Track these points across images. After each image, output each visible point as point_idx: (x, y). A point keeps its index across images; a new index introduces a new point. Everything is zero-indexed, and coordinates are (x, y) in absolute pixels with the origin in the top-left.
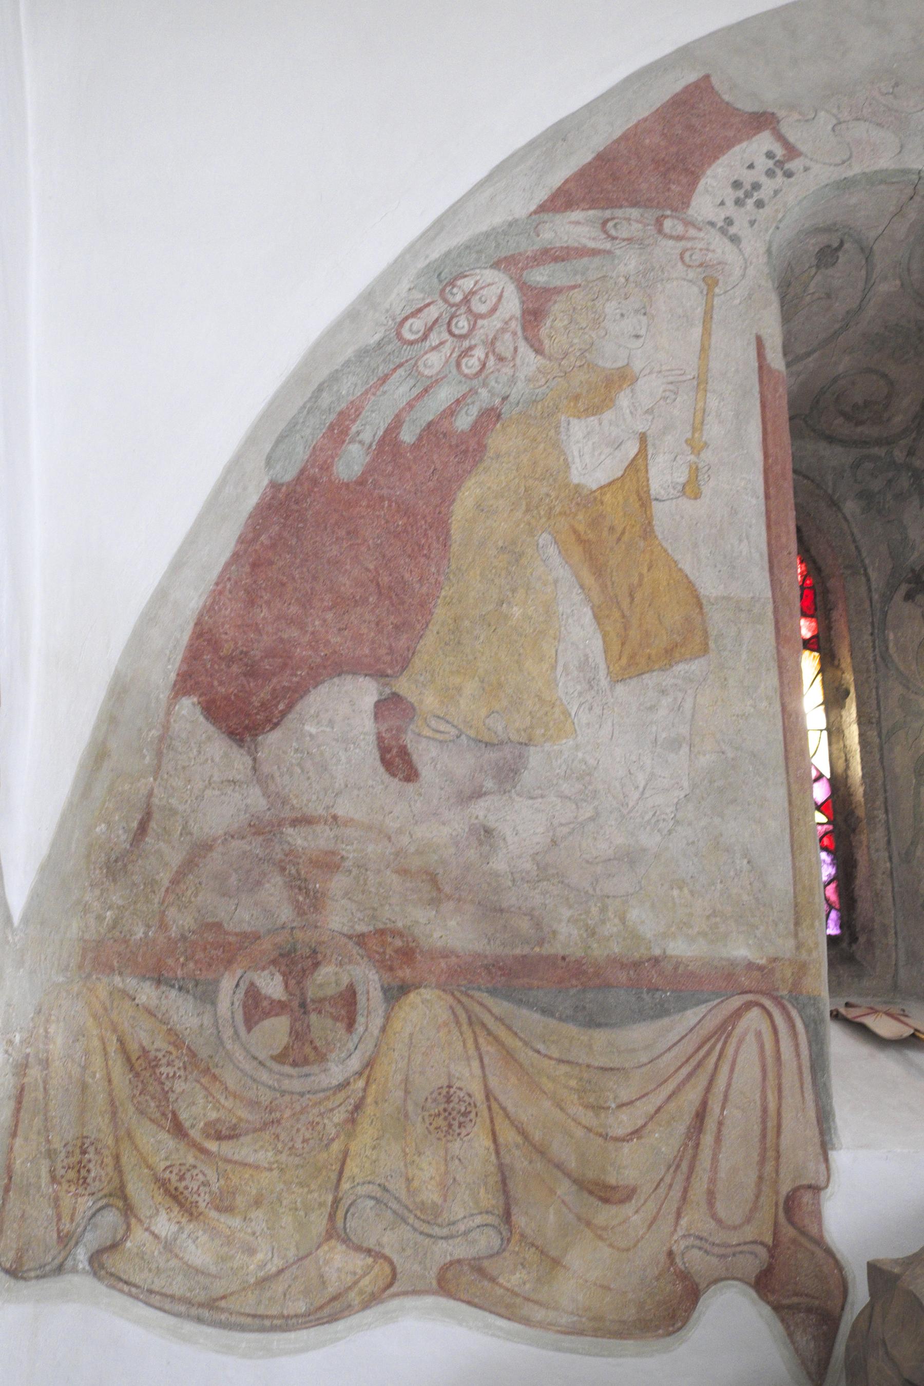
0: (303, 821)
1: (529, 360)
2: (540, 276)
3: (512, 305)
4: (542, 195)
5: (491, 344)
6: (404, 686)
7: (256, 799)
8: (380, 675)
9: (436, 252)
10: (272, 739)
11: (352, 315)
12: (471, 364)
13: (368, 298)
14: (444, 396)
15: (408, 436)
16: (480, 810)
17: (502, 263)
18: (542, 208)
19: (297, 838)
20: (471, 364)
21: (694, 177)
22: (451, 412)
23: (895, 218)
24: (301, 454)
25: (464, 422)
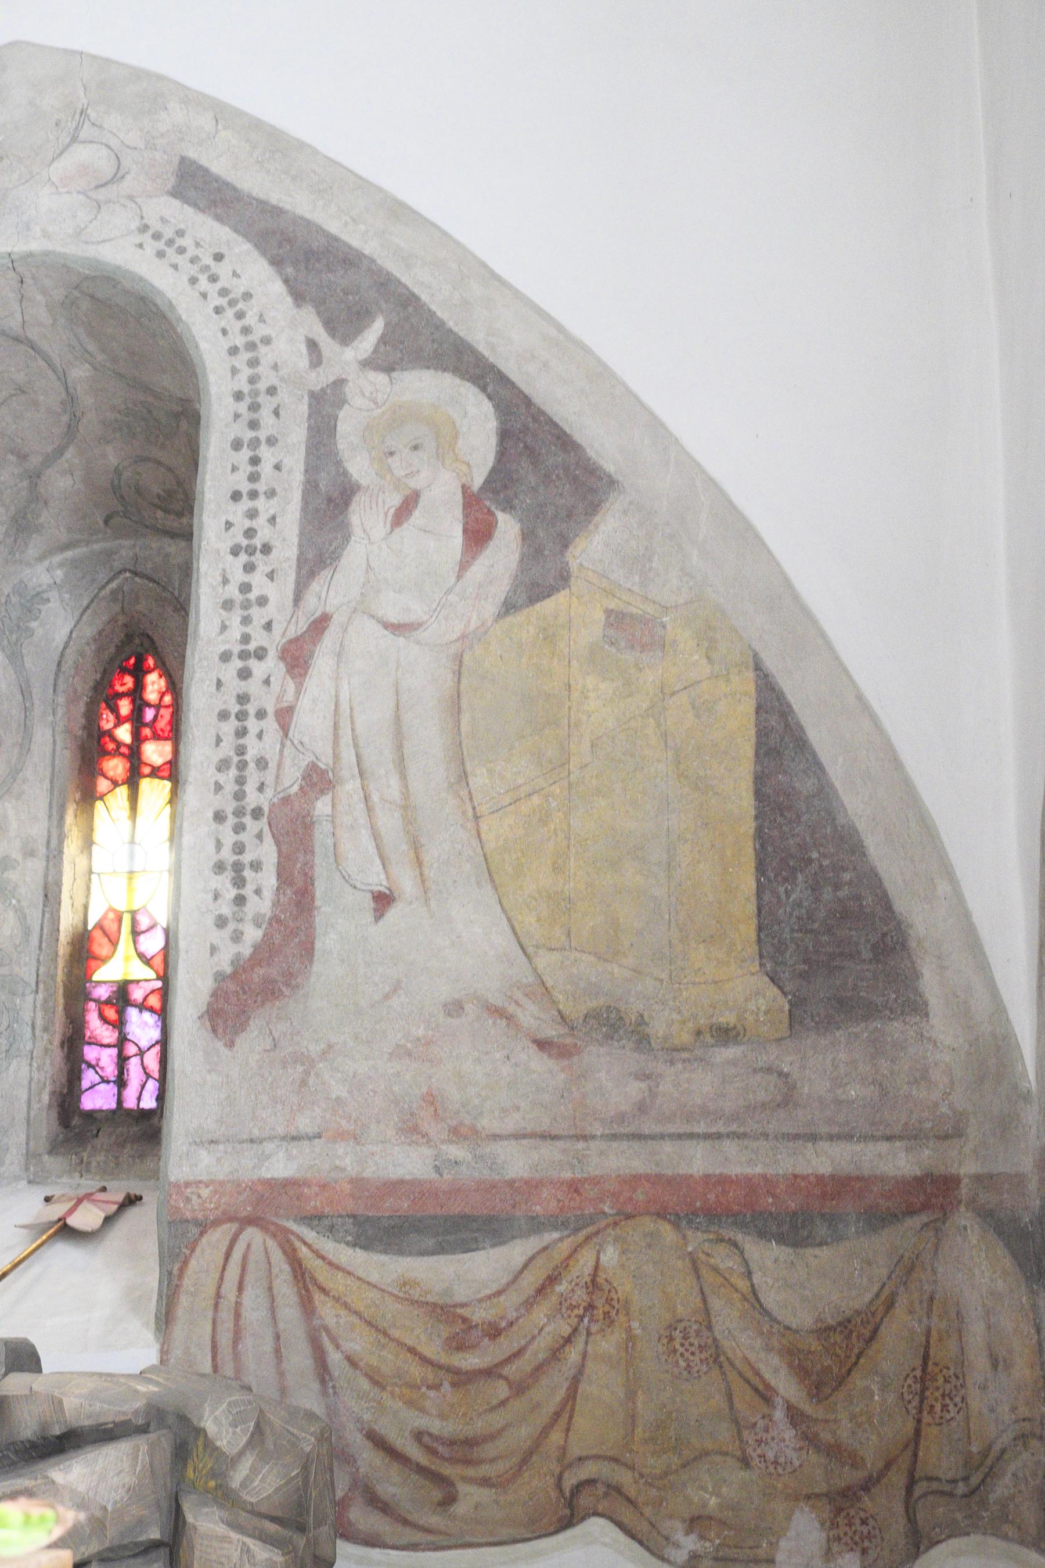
23: (24, 303)
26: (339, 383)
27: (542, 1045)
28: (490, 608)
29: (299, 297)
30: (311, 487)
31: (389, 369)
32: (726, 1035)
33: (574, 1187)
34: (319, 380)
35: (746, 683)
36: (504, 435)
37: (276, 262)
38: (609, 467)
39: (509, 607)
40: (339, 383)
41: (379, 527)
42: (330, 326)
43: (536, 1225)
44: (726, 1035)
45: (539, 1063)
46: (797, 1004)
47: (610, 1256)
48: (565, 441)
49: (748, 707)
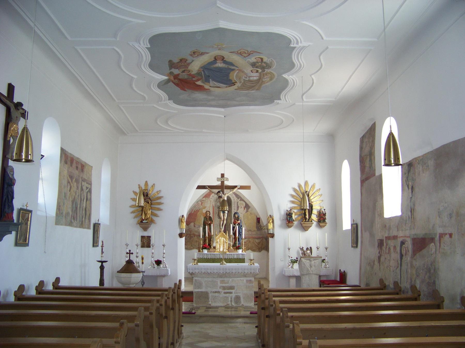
0: (190, 229)
1: (201, 206)
2: (202, 202)
3: (201, 203)
4: (203, 197)
5: (200, 206)
6: (195, 223)
7: (188, 228)
8: (194, 222)
9: (197, 201)
10: (189, 225)
11: (193, 205)
12: (199, 207)
13: (194, 204)
14: (197, 208)
15: (195, 210)
16: (198, 228)
17: (201, 201)
18: (203, 198)
19: (190, 230)
20: (199, 207)
21: (210, 195)
22: (198, 209)
24: (190, 212)
25: (198, 210)
26: (238, 202)
27: (247, 231)
28: (245, 213)
29: (236, 197)
30: (237, 206)
31: (240, 201)
32: (254, 231)
33: (249, 237)
34: (237, 201)
35: (256, 216)
36: (246, 204)
37: (235, 195)
38: (250, 206)
39: (246, 212)
40: (238, 202)
41: (240, 208)
42: (238, 199)
43: (247, 238)
44: (254, 231)
45: (247, 232)
46: (257, 230)
47: (250, 240)
48: (248, 205)
49: (256, 217)
